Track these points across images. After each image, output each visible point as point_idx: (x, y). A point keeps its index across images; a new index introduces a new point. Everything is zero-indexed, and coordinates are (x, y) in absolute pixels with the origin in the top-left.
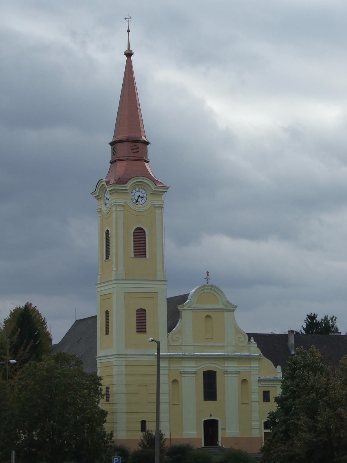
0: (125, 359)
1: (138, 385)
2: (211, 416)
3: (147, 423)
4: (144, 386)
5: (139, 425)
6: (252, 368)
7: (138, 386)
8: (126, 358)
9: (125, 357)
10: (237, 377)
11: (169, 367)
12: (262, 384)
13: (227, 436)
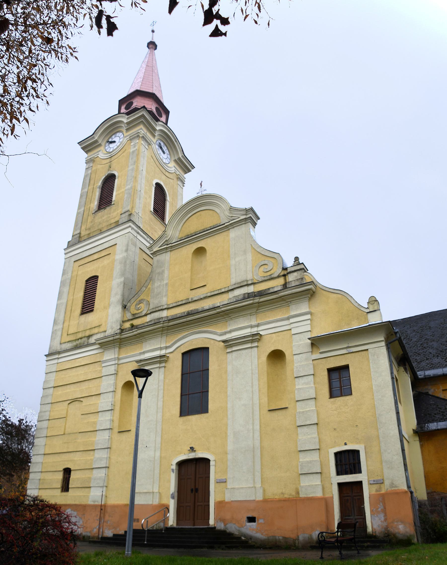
0: (56, 361)
1: (69, 402)
2: (192, 449)
3: (72, 473)
4: (77, 402)
5: (60, 476)
6: (292, 320)
7: (69, 404)
8: (58, 358)
9: (57, 356)
10: (256, 349)
11: (119, 359)
12: (321, 351)
13: (228, 498)
